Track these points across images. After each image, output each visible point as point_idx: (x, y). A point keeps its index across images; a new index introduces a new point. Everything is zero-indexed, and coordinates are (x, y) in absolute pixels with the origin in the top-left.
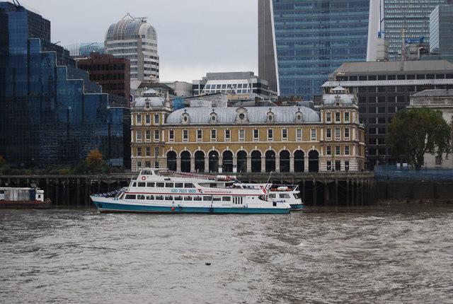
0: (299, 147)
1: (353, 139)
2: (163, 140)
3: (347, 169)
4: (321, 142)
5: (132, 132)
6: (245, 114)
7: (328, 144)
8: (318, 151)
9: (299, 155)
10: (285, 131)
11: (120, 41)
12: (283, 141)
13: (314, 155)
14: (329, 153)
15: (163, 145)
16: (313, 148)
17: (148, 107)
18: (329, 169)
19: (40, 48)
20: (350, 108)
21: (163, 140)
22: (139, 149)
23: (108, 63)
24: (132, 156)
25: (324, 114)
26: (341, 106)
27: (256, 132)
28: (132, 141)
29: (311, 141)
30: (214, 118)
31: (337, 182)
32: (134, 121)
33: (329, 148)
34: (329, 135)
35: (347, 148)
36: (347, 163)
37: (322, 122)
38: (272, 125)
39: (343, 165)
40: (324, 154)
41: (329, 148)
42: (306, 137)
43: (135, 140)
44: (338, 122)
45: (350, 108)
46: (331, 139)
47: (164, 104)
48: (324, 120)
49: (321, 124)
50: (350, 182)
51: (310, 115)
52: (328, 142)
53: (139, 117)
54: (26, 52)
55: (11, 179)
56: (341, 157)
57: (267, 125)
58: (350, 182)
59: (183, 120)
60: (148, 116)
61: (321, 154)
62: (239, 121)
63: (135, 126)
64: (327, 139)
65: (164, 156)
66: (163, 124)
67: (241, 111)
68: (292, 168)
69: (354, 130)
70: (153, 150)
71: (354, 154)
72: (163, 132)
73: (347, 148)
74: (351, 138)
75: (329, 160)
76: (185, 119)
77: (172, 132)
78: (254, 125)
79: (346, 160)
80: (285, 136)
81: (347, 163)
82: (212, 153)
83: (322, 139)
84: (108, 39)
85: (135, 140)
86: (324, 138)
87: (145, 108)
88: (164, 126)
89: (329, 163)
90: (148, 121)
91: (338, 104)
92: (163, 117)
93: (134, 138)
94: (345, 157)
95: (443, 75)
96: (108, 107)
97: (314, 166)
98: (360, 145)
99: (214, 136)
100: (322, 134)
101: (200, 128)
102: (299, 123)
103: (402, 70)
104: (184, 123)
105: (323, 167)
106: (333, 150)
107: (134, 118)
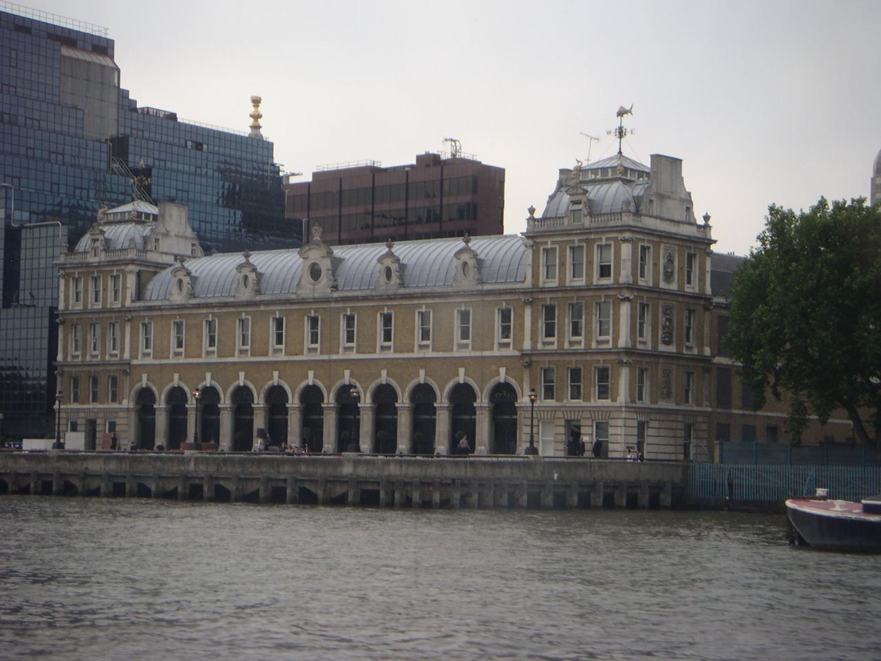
0: (462, 371)
4: (524, 355)
8: (518, 389)
9: (462, 397)
12: (417, 354)
13: (503, 398)
14: (549, 393)
15: (127, 369)
16: (502, 376)
21: (127, 356)
28: (60, 357)
29: (496, 352)
35: (603, 374)
37: (528, 284)
38: (390, 298)
42: (484, 341)
46: (554, 344)
48: (535, 275)
49: (525, 292)
56: (583, 409)
57: (381, 298)
59: (175, 290)
61: (524, 400)
62: (309, 289)
65: (127, 403)
66: (128, 303)
69: (625, 309)
71: (622, 397)
73: (603, 374)
74: (616, 339)
81: (601, 428)
83: (527, 345)
85: (65, 355)
86: (534, 340)
88: (130, 311)
92: (131, 281)
97: (504, 437)
104: (177, 298)
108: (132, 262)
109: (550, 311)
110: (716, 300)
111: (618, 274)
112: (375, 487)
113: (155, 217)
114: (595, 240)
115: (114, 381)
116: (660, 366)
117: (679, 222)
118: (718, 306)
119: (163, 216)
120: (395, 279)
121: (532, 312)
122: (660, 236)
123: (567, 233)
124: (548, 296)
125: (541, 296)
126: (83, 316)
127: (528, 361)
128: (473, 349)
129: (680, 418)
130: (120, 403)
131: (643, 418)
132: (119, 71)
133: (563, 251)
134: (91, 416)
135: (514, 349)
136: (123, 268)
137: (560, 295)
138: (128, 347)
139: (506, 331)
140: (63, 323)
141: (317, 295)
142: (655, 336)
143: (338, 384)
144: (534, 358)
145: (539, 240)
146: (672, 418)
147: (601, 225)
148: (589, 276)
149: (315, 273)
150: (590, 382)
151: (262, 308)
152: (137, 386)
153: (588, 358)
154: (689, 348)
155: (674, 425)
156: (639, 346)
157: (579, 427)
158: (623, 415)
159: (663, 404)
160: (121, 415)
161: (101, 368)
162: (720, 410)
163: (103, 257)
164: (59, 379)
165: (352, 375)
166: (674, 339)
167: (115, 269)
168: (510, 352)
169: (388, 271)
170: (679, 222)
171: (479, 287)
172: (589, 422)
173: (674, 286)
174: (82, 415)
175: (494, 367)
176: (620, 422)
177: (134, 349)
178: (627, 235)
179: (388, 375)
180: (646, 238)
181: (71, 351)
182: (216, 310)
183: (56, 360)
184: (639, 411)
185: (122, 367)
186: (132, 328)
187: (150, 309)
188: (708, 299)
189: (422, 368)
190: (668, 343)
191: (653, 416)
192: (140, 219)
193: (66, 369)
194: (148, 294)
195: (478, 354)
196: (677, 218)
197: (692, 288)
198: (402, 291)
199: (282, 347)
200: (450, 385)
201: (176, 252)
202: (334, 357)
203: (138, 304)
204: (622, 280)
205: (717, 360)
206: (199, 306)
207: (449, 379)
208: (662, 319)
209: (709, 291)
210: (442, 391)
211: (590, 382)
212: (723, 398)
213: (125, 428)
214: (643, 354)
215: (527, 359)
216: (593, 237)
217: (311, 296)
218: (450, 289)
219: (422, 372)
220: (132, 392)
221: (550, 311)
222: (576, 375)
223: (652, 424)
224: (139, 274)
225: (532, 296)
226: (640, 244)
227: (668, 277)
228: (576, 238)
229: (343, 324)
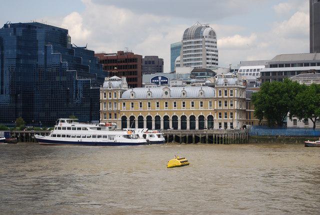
0: (201, 113)
1: (236, 108)
2: (119, 109)
3: (232, 127)
6: (168, 92)
10: (193, 103)
11: (188, 41)
13: (211, 118)
15: (119, 112)
17: (110, 87)
18: (220, 127)
19: (52, 51)
20: (233, 87)
23: (116, 58)
26: (228, 86)
27: (175, 103)
28: (101, 109)
30: (149, 94)
33: (220, 114)
34: (220, 105)
35: (232, 114)
36: (232, 124)
37: (216, 97)
39: (229, 125)
41: (220, 114)
42: (206, 107)
44: (226, 97)
47: (120, 86)
48: (217, 95)
50: (215, 136)
51: (209, 91)
52: (220, 110)
53: (105, 94)
54: (43, 54)
55: (21, 133)
58: (215, 136)
60: (110, 93)
61: (215, 118)
62: (165, 96)
63: (102, 100)
64: (219, 108)
65: (120, 119)
66: (119, 98)
67: (166, 90)
68: (197, 127)
69: (236, 102)
70: (113, 115)
72: (119, 103)
73: (232, 114)
75: (220, 121)
76: (132, 95)
77: (124, 104)
78: (174, 99)
80: (166, 106)
81: (232, 124)
83: (216, 108)
84: (184, 39)
87: (109, 89)
88: (119, 100)
89: (220, 124)
90: (110, 97)
93: (102, 108)
95: (289, 64)
96: (91, 88)
97: (211, 125)
99: (149, 106)
100: (216, 105)
101: (141, 102)
102: (202, 100)
103: (314, 60)
104: (132, 98)
105: (216, 126)
106: (223, 115)
107: (102, 95)
108: (120, 90)
109: (220, 102)
111: (234, 95)
115: (115, 114)
123: (223, 87)
127: (216, 111)
138: (119, 107)
139: (211, 106)
149: (166, 93)
159: (240, 119)
163: (112, 88)
168: (211, 109)
169: (184, 93)
177: (121, 108)
181: (104, 108)
184: (238, 120)
197: (243, 97)
221: (220, 102)
222: (226, 114)
225: (217, 99)
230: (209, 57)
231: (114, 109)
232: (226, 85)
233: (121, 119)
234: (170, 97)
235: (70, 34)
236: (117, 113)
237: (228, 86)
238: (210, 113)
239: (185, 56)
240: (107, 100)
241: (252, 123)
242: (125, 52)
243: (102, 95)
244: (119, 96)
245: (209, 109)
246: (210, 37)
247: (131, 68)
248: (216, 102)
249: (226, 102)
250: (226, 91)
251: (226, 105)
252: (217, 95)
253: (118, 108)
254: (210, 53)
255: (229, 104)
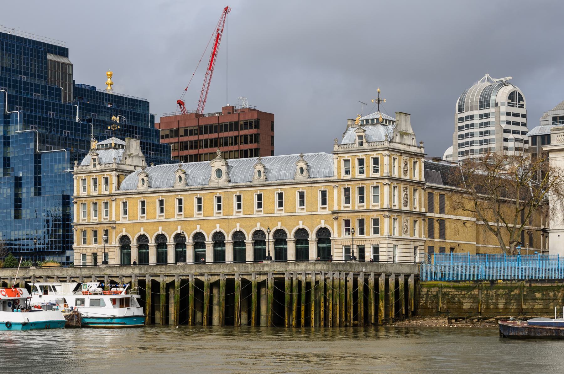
0: (301, 222)
2: (113, 219)
5: (75, 205)
7: (346, 216)
9: (301, 236)
12: (277, 214)
13: (324, 236)
22: (84, 233)
24: (75, 246)
25: (339, 162)
28: (75, 220)
31: (270, 279)
32: (78, 191)
33: (347, 223)
34: (347, 200)
35: (376, 222)
36: (376, 250)
37: (335, 178)
40: (340, 235)
41: (347, 223)
43: (78, 220)
45: (379, 150)
46: (350, 207)
48: (339, 173)
59: (140, 183)
61: (334, 235)
64: (344, 207)
66: (114, 192)
70: (101, 236)
74: (382, 203)
79: (375, 243)
81: (376, 250)
82: (178, 236)
83: (336, 208)
85: (78, 220)
86: (339, 206)
91: (361, 144)
93: (78, 215)
94: (370, 240)
97: (325, 254)
98: (431, 220)
104: (141, 188)
107: (78, 184)
110: (427, 184)
111: (383, 172)
112: (282, 276)
113: (123, 146)
114: (370, 155)
115: (107, 232)
116: (403, 217)
117: (410, 145)
118: (428, 187)
119: (129, 146)
120: (263, 176)
121: (338, 192)
122: (401, 153)
124: (346, 183)
125: (342, 183)
126: (88, 199)
128: (307, 211)
129: (412, 243)
130: (111, 244)
131: (396, 243)
132: (72, 65)
133: (354, 160)
134: (94, 251)
135: (329, 210)
136: (110, 173)
137: (352, 183)
139: (324, 202)
140: (76, 203)
141: (220, 185)
142: (400, 202)
143: (233, 231)
144: (340, 215)
145: (340, 155)
146: (409, 243)
147: (374, 147)
148: (368, 173)
150: (369, 226)
151: (190, 192)
152: (120, 235)
153: (368, 214)
154: (415, 208)
155: (409, 247)
156: (393, 207)
157: (364, 248)
158: (387, 242)
159: (404, 236)
160: (111, 250)
161: (99, 226)
162: (429, 239)
163: (98, 167)
164: (75, 232)
165: (240, 226)
166: (409, 204)
167: (105, 173)
168: (327, 212)
170: (410, 145)
171: (309, 180)
172: (369, 246)
173: (408, 177)
174: (89, 250)
175: (318, 220)
176: (385, 245)
177: (118, 215)
178: (386, 152)
179: (261, 225)
180: (395, 154)
181: (81, 217)
182: (164, 194)
183: (73, 222)
185: (111, 225)
186: (116, 204)
187: (126, 194)
188: (424, 184)
189: (279, 221)
190: (406, 206)
191: (400, 242)
192: (116, 147)
193: (79, 227)
194: (122, 186)
195: (310, 213)
196: (409, 143)
197: (417, 178)
198: (267, 182)
199: (202, 212)
200: (295, 230)
201: (135, 164)
202: (231, 217)
203: (118, 192)
204: (385, 175)
205: (429, 214)
206: (154, 192)
207: (294, 226)
208: (403, 194)
209: (423, 179)
210: (290, 233)
211: (369, 226)
212: (431, 234)
213: (113, 257)
214: (395, 212)
215: (335, 215)
216: (369, 153)
217: (217, 186)
218: (293, 181)
219: (279, 224)
220: (118, 238)
223: (399, 246)
224: (118, 177)
226: (392, 157)
227: (405, 172)
228: (360, 154)
229: (235, 199)
230: (511, 144)
231: (104, 218)
232: (361, 144)
233: (117, 244)
234: (227, 184)
235: (72, 59)
236: (110, 230)
237: (365, 145)
238: (323, 222)
239: (462, 145)
240: (100, 196)
241: (452, 249)
242: (237, 108)
243: (78, 184)
244: (114, 186)
245: (320, 212)
246: (510, 105)
247: (246, 142)
248: (336, 191)
249: (361, 190)
250: (361, 162)
251: (362, 199)
252: (339, 173)
253: (111, 217)
254: (511, 136)
255: (369, 194)
